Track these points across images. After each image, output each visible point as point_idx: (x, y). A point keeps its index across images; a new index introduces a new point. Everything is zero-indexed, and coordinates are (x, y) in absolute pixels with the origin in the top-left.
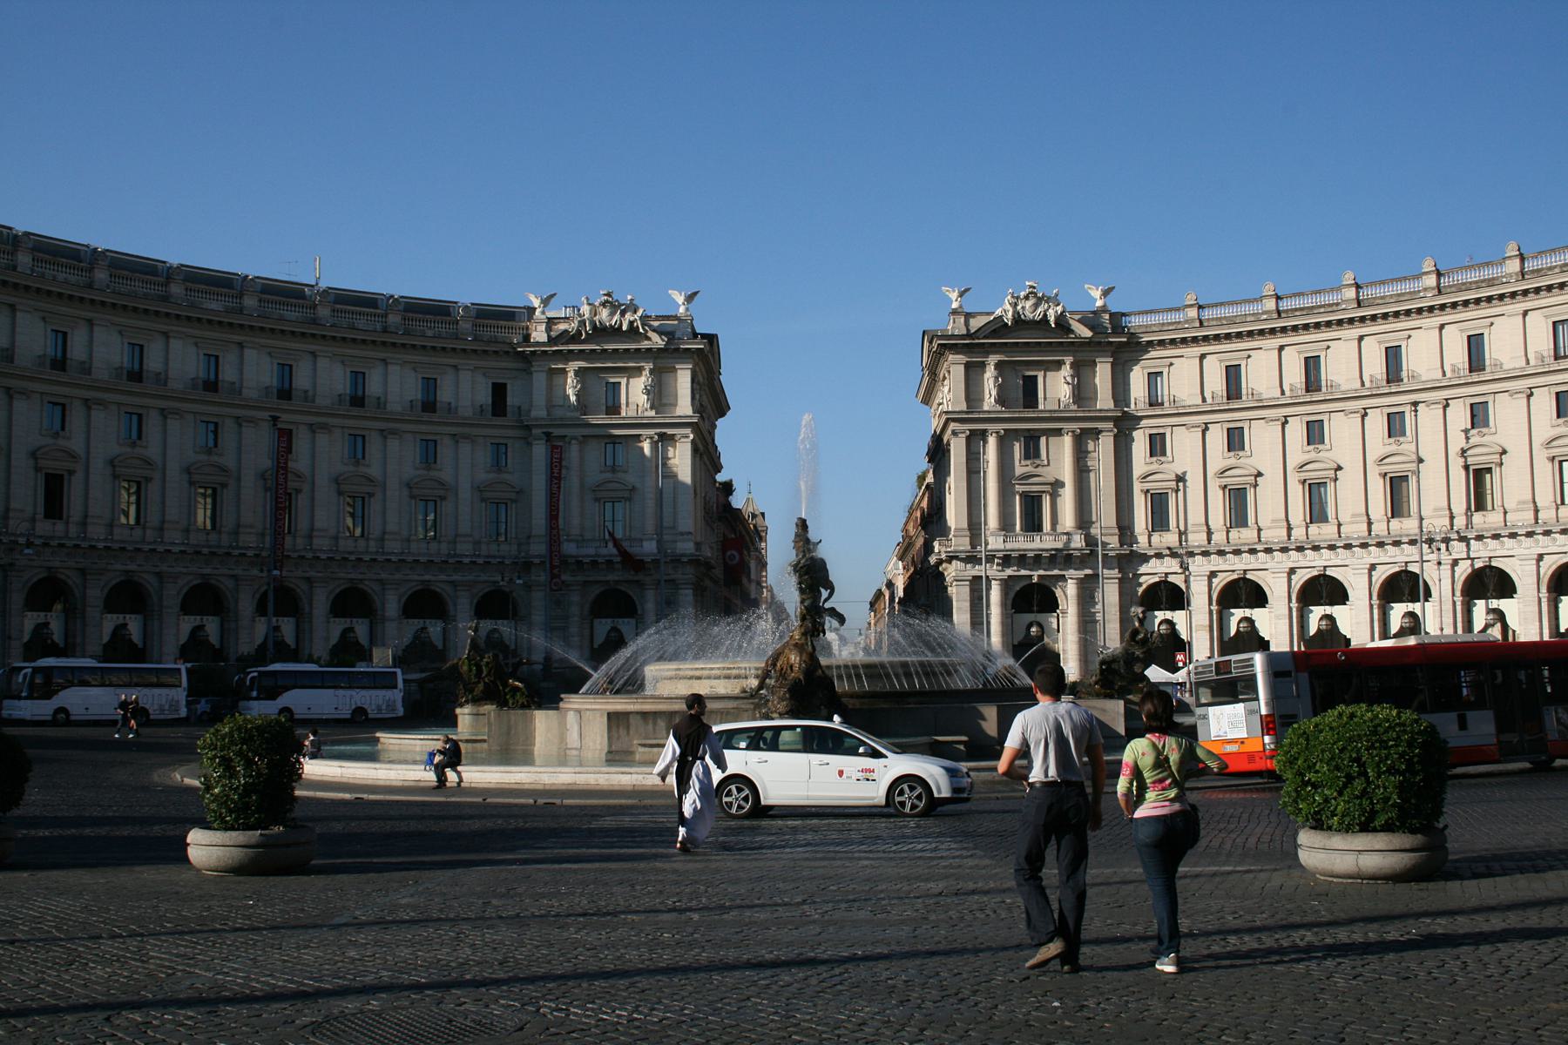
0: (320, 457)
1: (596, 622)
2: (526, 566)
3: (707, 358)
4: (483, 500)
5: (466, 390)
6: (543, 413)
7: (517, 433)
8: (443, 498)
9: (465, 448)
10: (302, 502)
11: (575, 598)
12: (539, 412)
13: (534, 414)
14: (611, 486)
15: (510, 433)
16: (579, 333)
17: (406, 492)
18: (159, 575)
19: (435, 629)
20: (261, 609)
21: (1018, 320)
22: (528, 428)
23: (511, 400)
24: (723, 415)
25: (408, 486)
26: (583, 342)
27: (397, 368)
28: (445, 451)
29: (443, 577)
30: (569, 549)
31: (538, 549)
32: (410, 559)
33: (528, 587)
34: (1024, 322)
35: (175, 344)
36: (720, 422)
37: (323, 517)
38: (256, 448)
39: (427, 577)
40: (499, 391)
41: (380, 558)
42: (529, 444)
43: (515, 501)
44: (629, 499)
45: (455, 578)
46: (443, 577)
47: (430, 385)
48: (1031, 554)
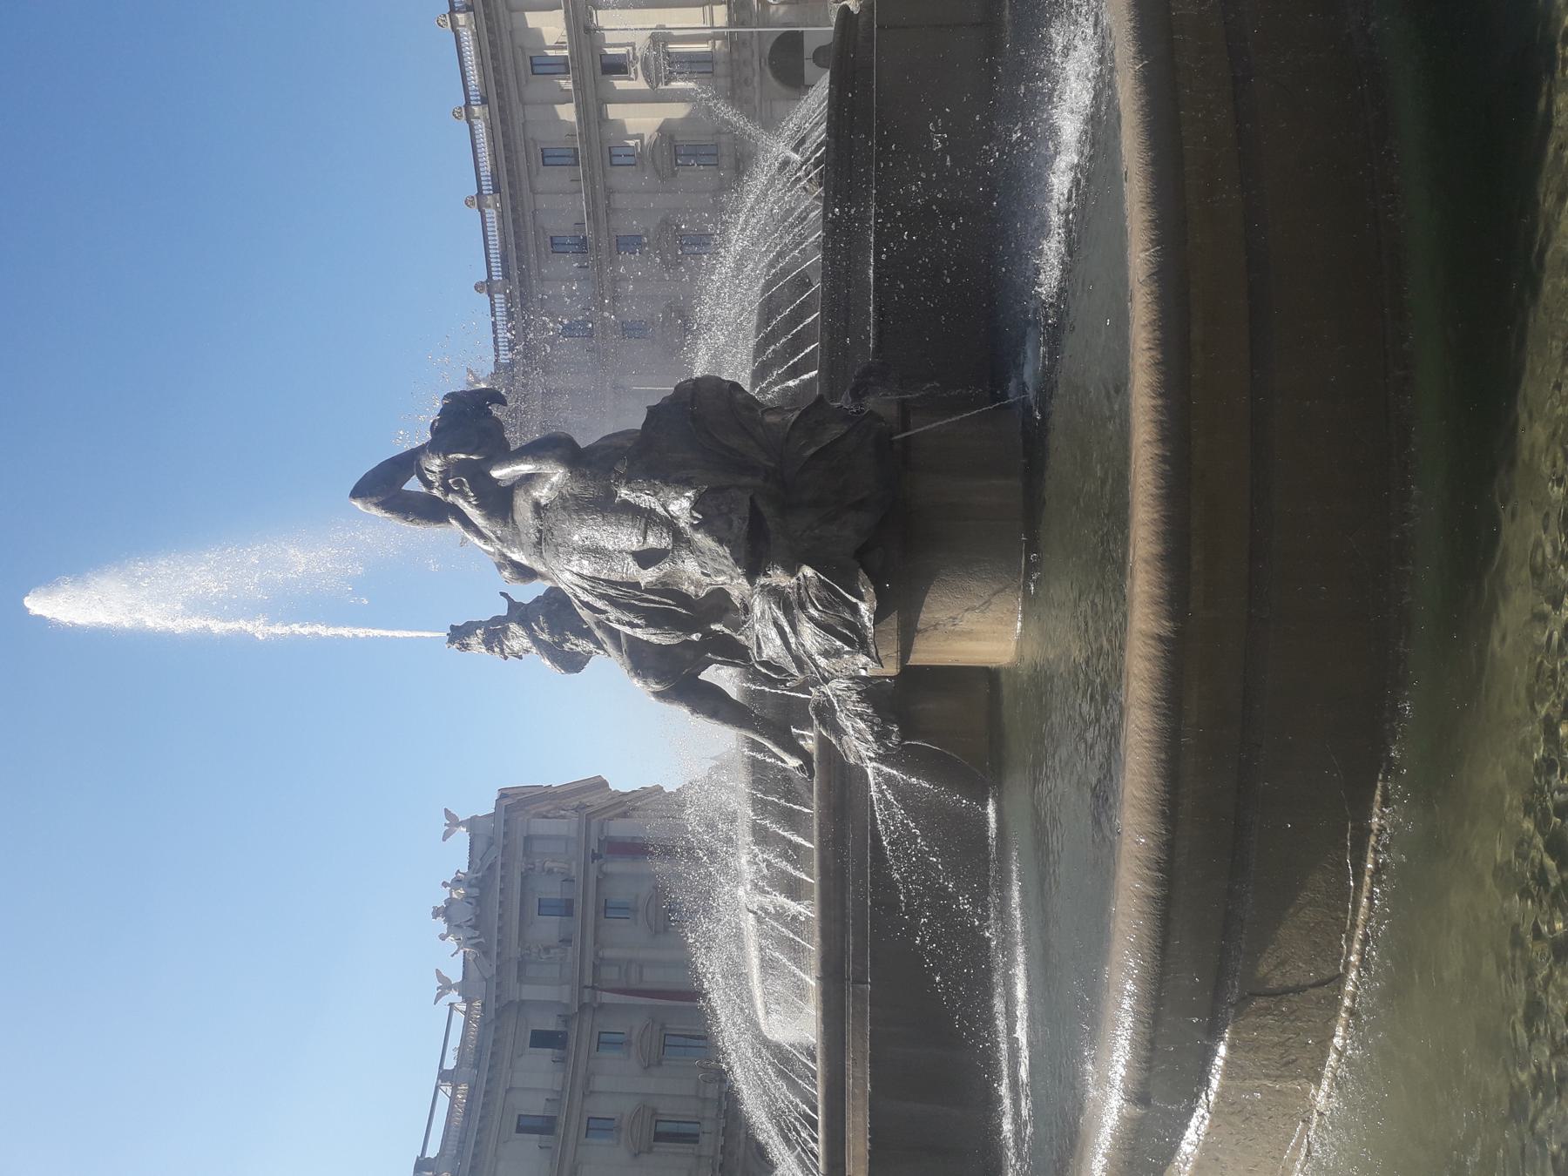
3: (514, 803)
16: (476, 946)
22: (582, 1007)
23: (550, 1024)
24: (604, 784)
28: (603, 1107)
32: (720, 1157)
36: (614, 786)
42: (602, 1006)
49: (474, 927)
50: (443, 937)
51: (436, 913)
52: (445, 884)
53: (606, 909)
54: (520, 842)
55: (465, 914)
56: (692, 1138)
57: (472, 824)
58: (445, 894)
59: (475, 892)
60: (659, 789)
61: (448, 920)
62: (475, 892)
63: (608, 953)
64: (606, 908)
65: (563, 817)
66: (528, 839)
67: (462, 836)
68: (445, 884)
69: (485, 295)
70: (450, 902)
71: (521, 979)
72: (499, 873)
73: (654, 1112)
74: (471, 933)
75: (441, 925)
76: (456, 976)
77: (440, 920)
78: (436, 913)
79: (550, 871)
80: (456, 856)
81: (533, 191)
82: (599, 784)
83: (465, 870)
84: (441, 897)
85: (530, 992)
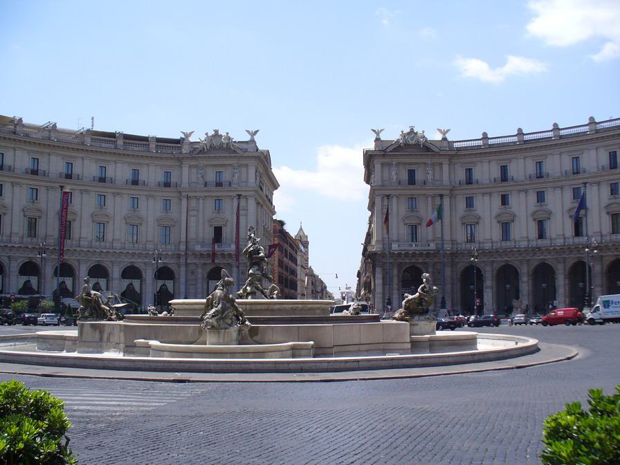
0: (84, 206)
1: (210, 281)
2: (179, 256)
3: (264, 160)
5: (152, 174)
7: (175, 195)
10: (75, 225)
11: (200, 271)
12: (185, 184)
15: (172, 195)
18: (9, 257)
19: (136, 284)
20: (55, 274)
21: (407, 145)
22: (180, 192)
24: (276, 188)
29: (140, 260)
30: (198, 248)
31: (183, 247)
33: (179, 266)
35: (19, 153)
36: (275, 192)
37: (84, 231)
38: (55, 198)
39: (132, 260)
40: (168, 174)
41: (111, 251)
42: (180, 200)
43: (173, 226)
46: (140, 260)
47: (136, 172)
48: (410, 252)
49: (211, 146)
51: (216, 131)
52: (227, 133)
54: (245, 162)
57: (253, 141)
58: (224, 134)
59: (225, 146)
60: (274, 213)
61: (213, 136)
62: (225, 146)
63: (201, 201)
65: (256, 179)
66: (247, 166)
67: (248, 138)
68: (227, 133)
70: (221, 136)
73: (141, 224)
74: (208, 145)
75: (211, 133)
76: (192, 139)
77: (213, 133)
78: (216, 131)
80: (239, 136)
82: (275, 185)
84: (222, 132)
85: (185, 170)
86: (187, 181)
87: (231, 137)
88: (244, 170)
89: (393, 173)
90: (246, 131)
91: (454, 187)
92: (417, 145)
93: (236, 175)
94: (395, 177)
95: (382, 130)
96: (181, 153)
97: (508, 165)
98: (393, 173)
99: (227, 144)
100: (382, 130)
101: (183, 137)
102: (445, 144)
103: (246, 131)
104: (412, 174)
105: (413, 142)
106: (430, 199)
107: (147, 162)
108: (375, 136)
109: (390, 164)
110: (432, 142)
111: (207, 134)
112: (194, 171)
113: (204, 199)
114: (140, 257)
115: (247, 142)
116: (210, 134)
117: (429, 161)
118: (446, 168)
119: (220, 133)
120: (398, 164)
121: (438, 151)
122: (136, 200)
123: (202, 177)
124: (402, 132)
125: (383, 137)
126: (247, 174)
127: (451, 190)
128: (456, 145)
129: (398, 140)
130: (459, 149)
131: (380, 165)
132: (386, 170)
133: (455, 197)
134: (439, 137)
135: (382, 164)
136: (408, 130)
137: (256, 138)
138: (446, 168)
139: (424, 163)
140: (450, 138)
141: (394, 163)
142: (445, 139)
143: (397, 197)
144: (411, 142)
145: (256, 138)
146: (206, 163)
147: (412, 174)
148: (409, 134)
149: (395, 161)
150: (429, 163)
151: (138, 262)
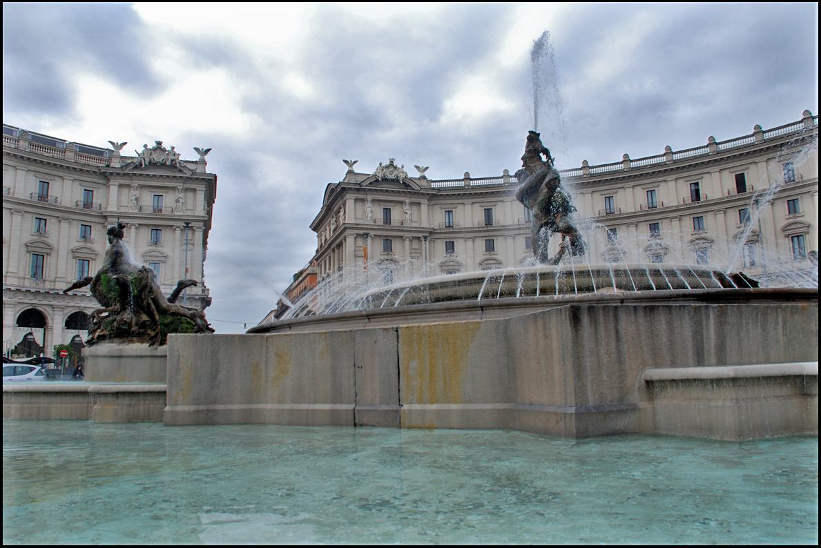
4: (74, 257)
6: (115, 209)
8: (48, 254)
9: (65, 225)
13: (109, 209)
14: (153, 254)
15: (94, 219)
17: (25, 249)
19: (38, 334)
22: (105, 217)
25: (27, 245)
26: (143, 170)
27: (24, 173)
32: (24, 289)
34: (386, 179)
44: (164, 262)
45: (53, 303)
49: (150, 163)
50: (145, 146)
51: (159, 143)
52: (173, 148)
53: (156, 229)
54: (193, 186)
55: (157, 157)
56: (34, 275)
59: (168, 163)
61: (155, 149)
62: (168, 163)
64: (157, 230)
69: (463, 177)
70: (164, 150)
71: (121, 186)
72: (178, 175)
74: (147, 161)
75: (152, 145)
76: (123, 153)
79: (177, 201)
81: (512, 202)
83: (180, 158)
84: (166, 145)
85: (114, 189)
86: (116, 203)
87: (177, 152)
88: (190, 195)
89: (369, 210)
90: (195, 148)
91: (434, 229)
92: (396, 181)
93: (181, 200)
94: (370, 215)
95: (356, 162)
96: (108, 166)
97: (493, 208)
98: (369, 210)
99: (172, 161)
100: (356, 162)
101: (111, 148)
102: (424, 183)
103: (195, 148)
104: (387, 212)
105: (393, 177)
106: (407, 242)
107: (61, 174)
108: (346, 168)
109: (363, 200)
110: (411, 179)
111: (145, 146)
112: (125, 191)
113: (137, 228)
114: (45, 298)
115: (196, 162)
116: (150, 147)
117: (407, 201)
118: (424, 208)
119: (163, 145)
120: (374, 201)
121: (419, 188)
122: (43, 222)
123: (137, 199)
124: (381, 164)
125: (357, 169)
126: (195, 201)
127: (431, 233)
128: (433, 185)
129: (375, 175)
130: (439, 189)
131: (353, 201)
132: (359, 205)
133: (434, 242)
134: (417, 175)
135: (356, 200)
136: (388, 163)
137: (207, 158)
138: (424, 208)
139: (401, 203)
140: (430, 175)
141: (369, 199)
142: (424, 178)
143: (372, 238)
144: (390, 177)
145: (207, 158)
146: (142, 183)
147: (387, 212)
148: (387, 167)
149: (370, 198)
150: (407, 201)
151: (42, 304)
